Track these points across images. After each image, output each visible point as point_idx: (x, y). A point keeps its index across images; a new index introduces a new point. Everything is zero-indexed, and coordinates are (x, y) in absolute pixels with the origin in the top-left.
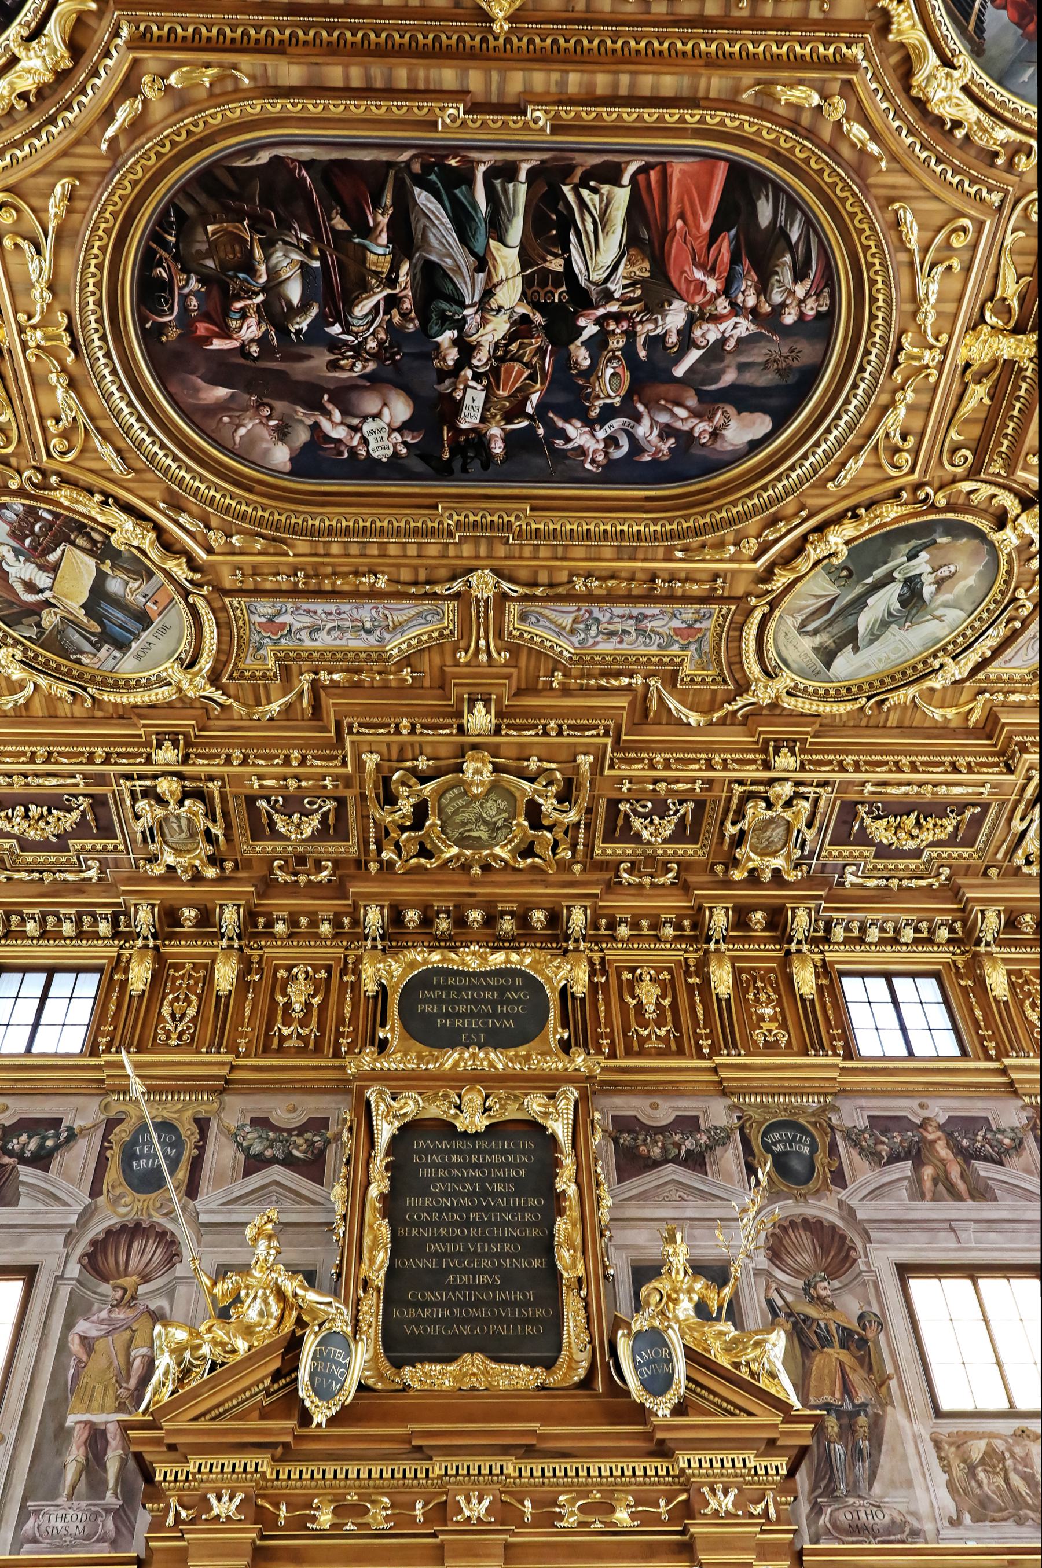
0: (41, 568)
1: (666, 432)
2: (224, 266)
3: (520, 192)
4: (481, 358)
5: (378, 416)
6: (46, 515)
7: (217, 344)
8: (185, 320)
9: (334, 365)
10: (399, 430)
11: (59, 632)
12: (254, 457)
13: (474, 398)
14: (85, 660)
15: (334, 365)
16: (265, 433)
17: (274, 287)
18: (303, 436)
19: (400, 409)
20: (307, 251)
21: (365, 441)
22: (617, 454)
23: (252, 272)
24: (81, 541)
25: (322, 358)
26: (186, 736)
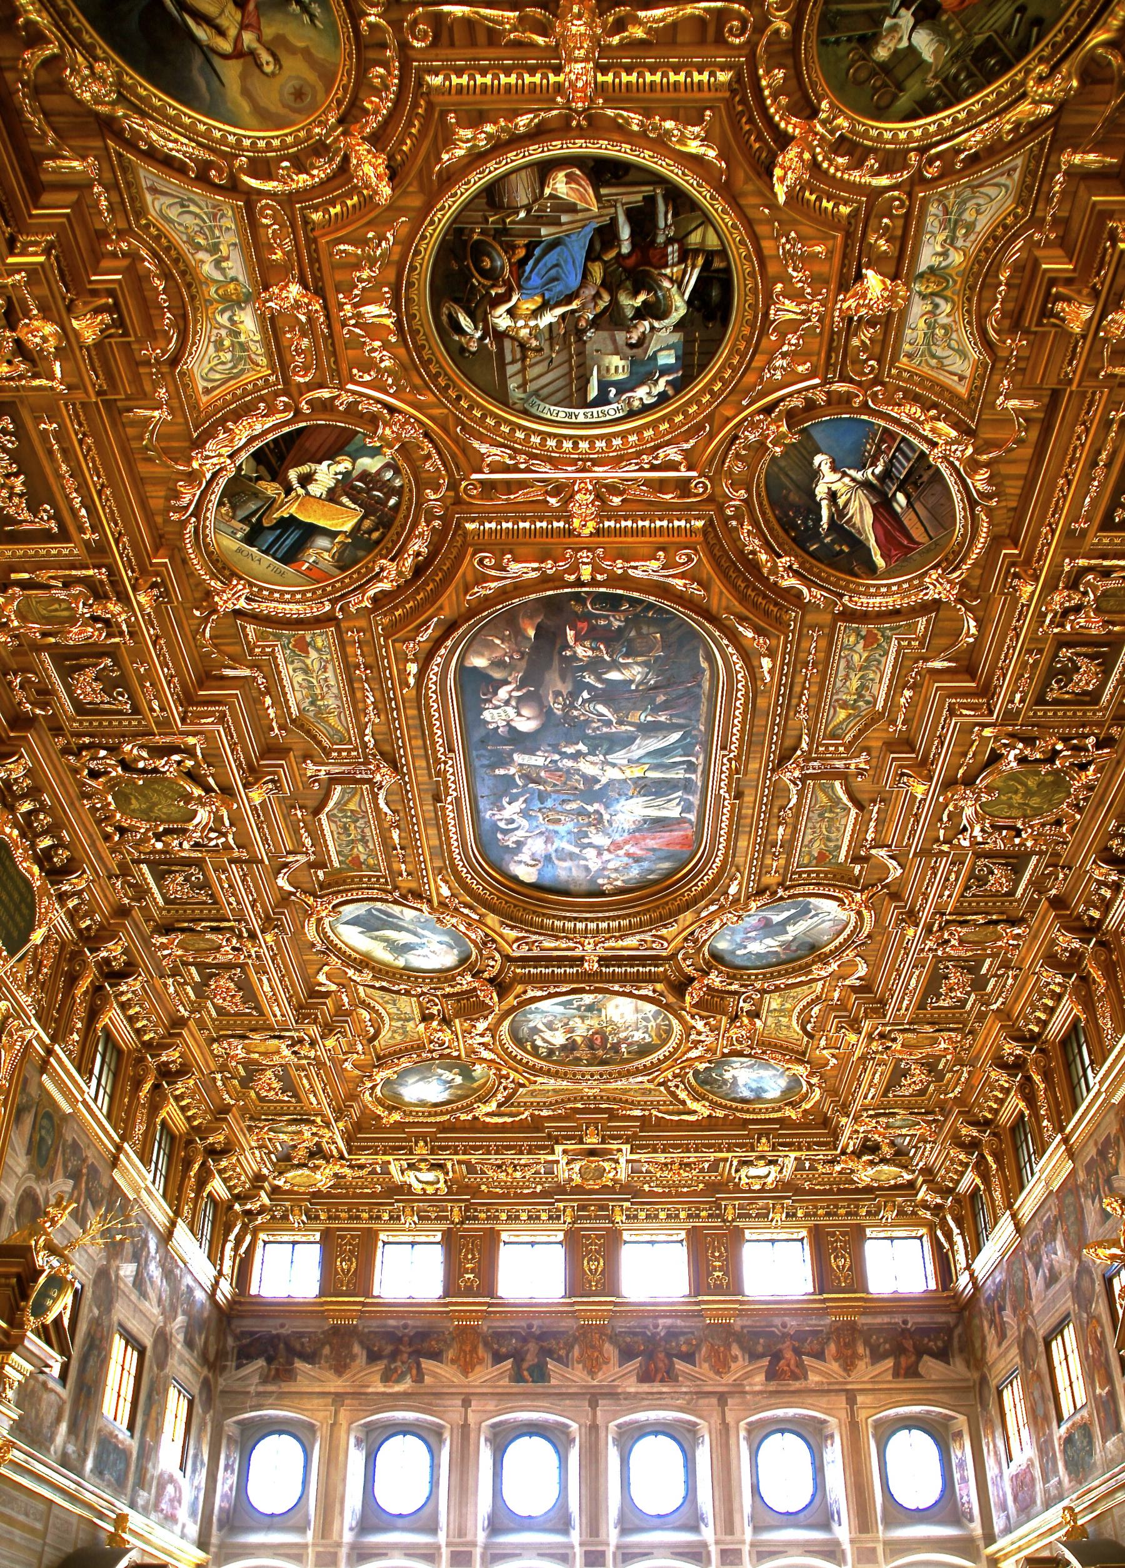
0: (331, 491)
1: (519, 844)
2: (630, 641)
3: (679, 774)
4: (568, 763)
5: (519, 714)
6: (392, 502)
7: (570, 634)
8: (588, 616)
9: (558, 694)
10: (508, 724)
11: (256, 495)
12: (475, 647)
13: (538, 760)
14: (223, 510)
15: (558, 694)
16: (497, 654)
17: (615, 666)
18: (497, 675)
19: (526, 725)
20: (641, 683)
21: (497, 707)
22: (502, 825)
23: (627, 655)
24: (367, 524)
25: (565, 688)
26: (170, 602)
